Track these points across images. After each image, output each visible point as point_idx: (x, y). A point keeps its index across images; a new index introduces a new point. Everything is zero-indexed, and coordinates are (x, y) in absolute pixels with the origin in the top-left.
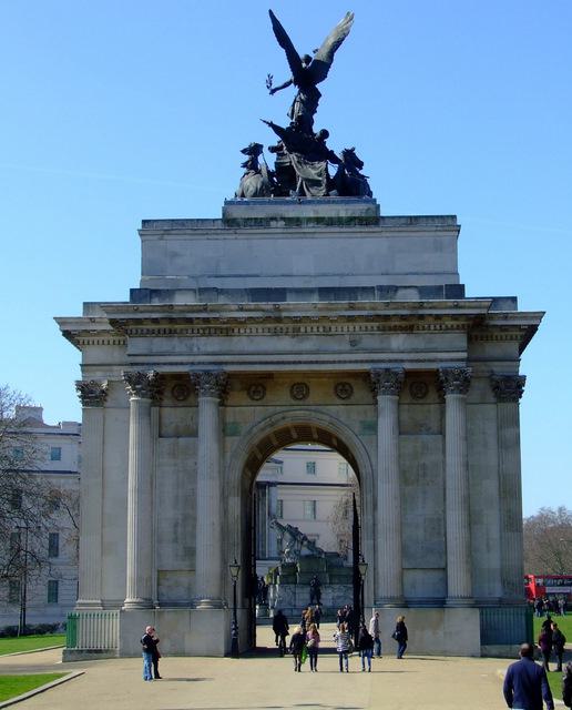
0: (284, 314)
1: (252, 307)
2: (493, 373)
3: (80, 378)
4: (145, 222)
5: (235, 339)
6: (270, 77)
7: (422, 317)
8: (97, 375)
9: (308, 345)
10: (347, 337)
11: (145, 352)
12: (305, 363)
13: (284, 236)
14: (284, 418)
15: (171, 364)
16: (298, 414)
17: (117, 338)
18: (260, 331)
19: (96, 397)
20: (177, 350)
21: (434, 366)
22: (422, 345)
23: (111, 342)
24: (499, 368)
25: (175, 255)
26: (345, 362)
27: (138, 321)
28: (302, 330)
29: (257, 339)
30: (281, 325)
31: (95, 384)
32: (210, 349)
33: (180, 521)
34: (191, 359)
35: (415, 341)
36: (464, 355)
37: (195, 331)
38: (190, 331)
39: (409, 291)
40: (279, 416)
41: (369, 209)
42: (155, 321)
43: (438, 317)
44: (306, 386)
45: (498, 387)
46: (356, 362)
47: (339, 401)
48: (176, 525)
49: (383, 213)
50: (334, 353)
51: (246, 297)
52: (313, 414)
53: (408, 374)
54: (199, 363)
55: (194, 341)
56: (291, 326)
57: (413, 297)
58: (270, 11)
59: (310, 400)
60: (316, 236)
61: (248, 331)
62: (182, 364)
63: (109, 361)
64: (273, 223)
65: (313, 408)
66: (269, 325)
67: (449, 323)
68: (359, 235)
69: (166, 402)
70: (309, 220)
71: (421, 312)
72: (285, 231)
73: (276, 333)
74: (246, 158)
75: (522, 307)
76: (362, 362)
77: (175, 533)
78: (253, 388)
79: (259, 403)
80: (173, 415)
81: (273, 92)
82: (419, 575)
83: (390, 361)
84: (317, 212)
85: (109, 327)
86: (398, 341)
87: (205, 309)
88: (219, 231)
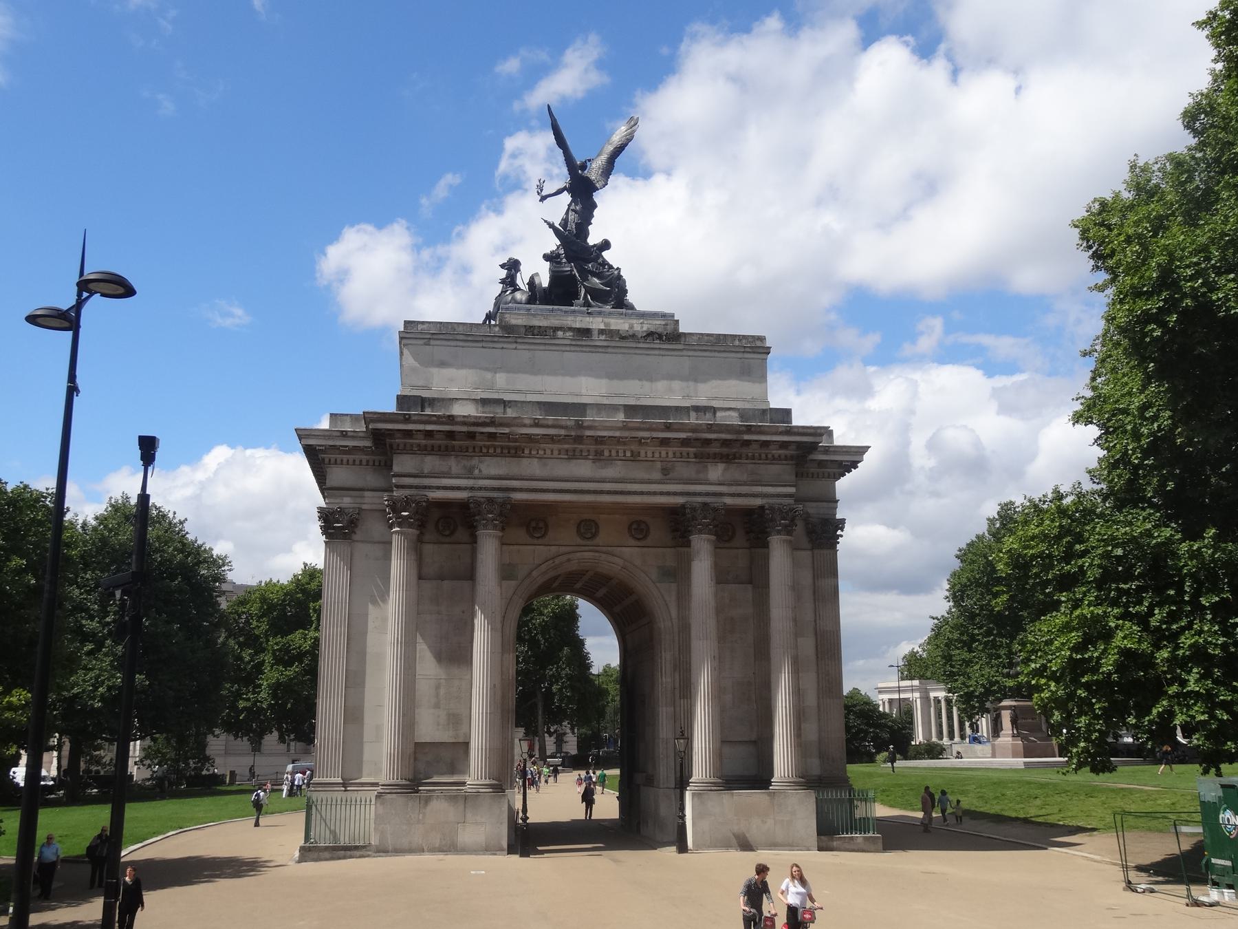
0: (588, 433)
1: (550, 423)
3: (324, 505)
4: (408, 323)
5: (525, 461)
7: (747, 443)
9: (609, 472)
10: (659, 465)
11: (413, 471)
12: (609, 492)
13: (573, 348)
15: (445, 488)
16: (583, 557)
17: (377, 458)
18: (556, 452)
23: (364, 462)
26: (655, 493)
27: (408, 434)
28: (606, 453)
30: (581, 446)
32: (493, 471)
34: (470, 483)
36: (792, 490)
39: (728, 413)
40: (565, 558)
42: (429, 434)
43: (766, 444)
44: (596, 524)
46: (668, 494)
47: (632, 542)
48: (438, 687)
49: (681, 330)
50: (642, 482)
51: (538, 412)
52: (604, 556)
54: (480, 489)
55: (475, 461)
56: (592, 448)
57: (733, 419)
59: (599, 540)
60: (610, 350)
61: (541, 452)
62: (459, 488)
63: (360, 484)
64: (560, 334)
65: (604, 549)
66: (566, 446)
67: (777, 452)
68: (657, 352)
69: (427, 537)
70: (601, 332)
71: (746, 437)
72: (574, 343)
73: (572, 456)
75: (839, 440)
76: (675, 494)
77: (437, 695)
78: (533, 524)
79: (540, 541)
81: (543, 199)
83: (708, 494)
84: (606, 324)
85: (368, 443)
86: (716, 472)
87: (492, 422)
88: (496, 339)
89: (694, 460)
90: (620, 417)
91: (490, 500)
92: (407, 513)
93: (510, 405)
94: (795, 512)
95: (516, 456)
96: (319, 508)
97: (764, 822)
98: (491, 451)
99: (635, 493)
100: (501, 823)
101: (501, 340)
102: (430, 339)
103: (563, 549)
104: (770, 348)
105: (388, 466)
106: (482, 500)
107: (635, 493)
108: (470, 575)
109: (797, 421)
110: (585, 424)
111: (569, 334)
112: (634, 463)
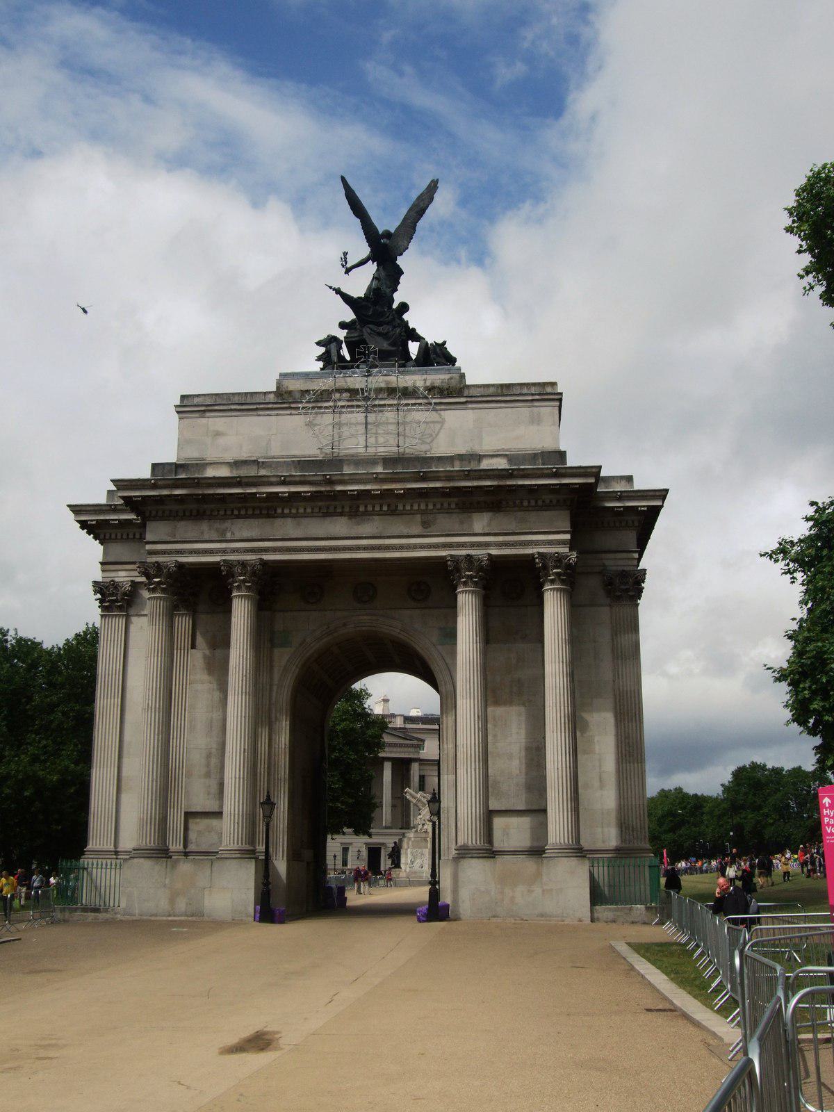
0: (339, 488)
2: (604, 565)
3: (100, 579)
4: (183, 397)
5: (279, 521)
6: (345, 254)
8: (123, 576)
9: (367, 528)
14: (345, 625)
16: (362, 620)
19: (116, 601)
20: (206, 537)
21: (529, 551)
24: (614, 563)
25: (218, 434)
27: (160, 500)
28: (362, 509)
29: (305, 521)
31: (115, 585)
32: (246, 534)
33: (214, 751)
34: (224, 545)
36: (568, 537)
37: (229, 512)
38: (222, 513)
41: (451, 378)
45: (610, 584)
48: (209, 756)
55: (228, 524)
57: (502, 464)
58: (343, 179)
61: (294, 511)
62: (211, 552)
66: (320, 504)
70: (379, 391)
72: (350, 404)
74: (323, 350)
75: (638, 485)
77: (208, 765)
81: (348, 271)
82: (514, 821)
84: (387, 383)
88: (270, 406)
89: (457, 510)
91: (243, 564)
92: (158, 580)
93: (264, 466)
94: (569, 560)
95: (268, 516)
96: (96, 584)
97: (530, 892)
98: (243, 512)
100: (248, 889)
101: (275, 406)
102: (204, 411)
104: (561, 394)
106: (235, 563)
109: (572, 461)
110: (334, 478)
111: (345, 395)
112: (395, 517)
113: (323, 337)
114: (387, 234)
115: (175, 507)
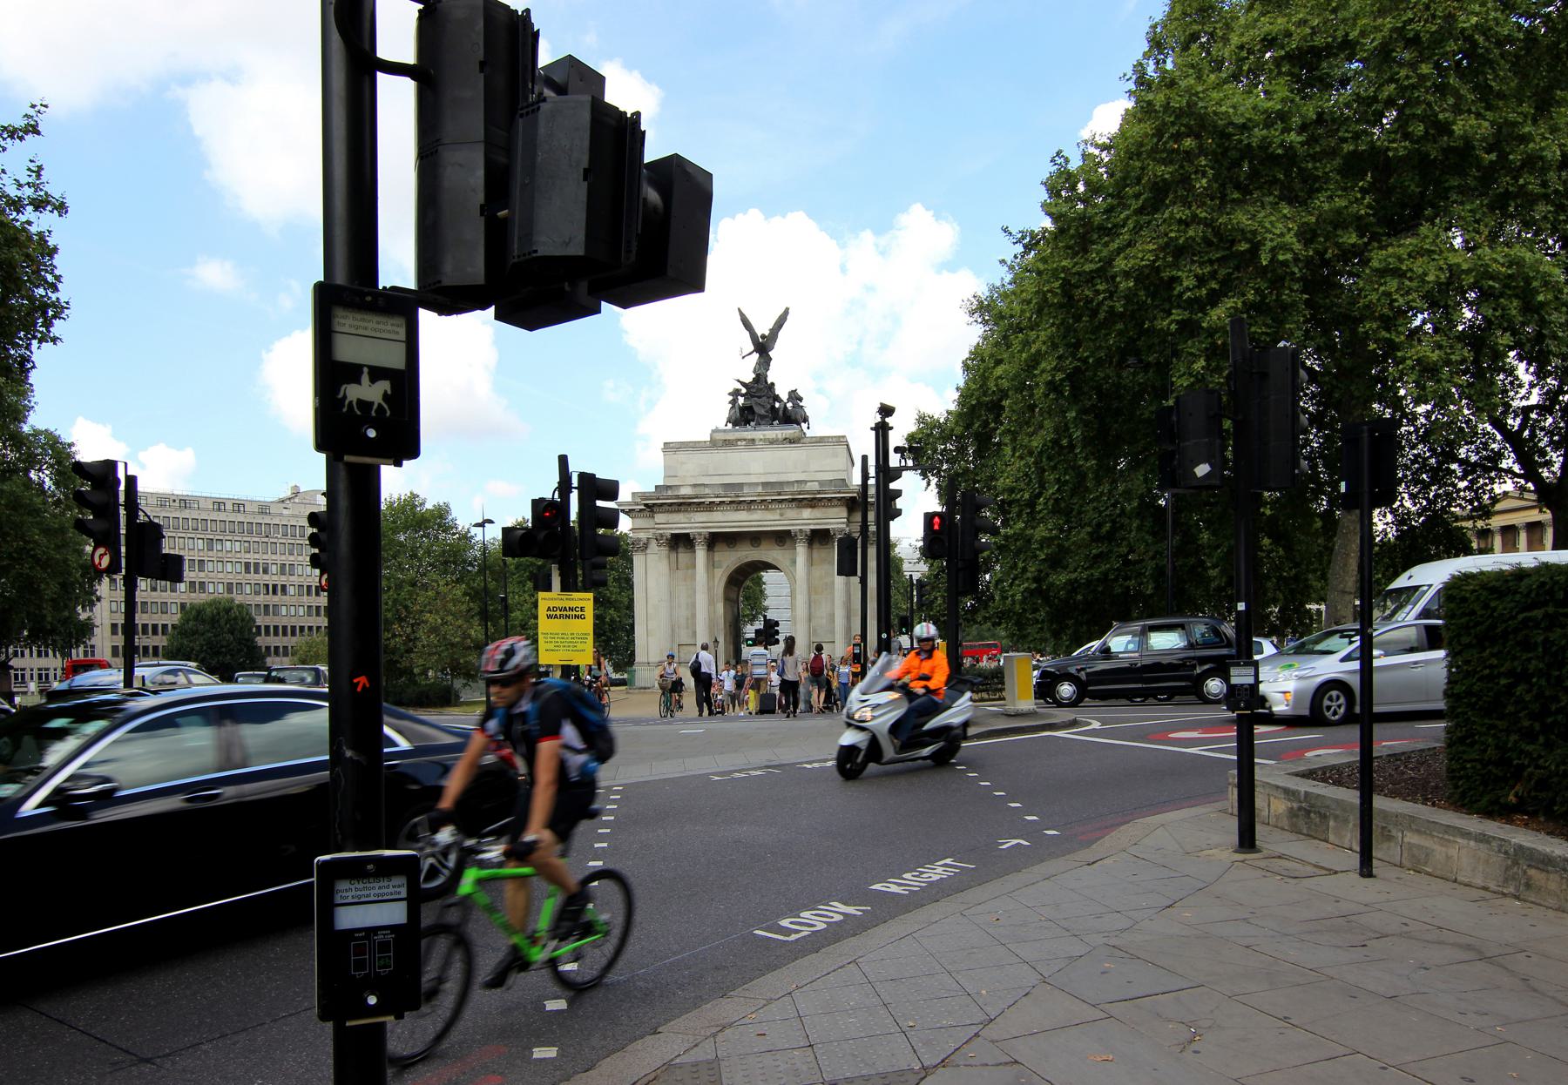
22: (819, 516)
25: (682, 463)
31: (639, 540)
32: (701, 520)
35: (817, 513)
48: (687, 619)
53: (812, 531)
57: (815, 486)
58: (739, 309)
62: (685, 528)
64: (739, 443)
69: (680, 550)
74: (731, 398)
80: (683, 556)
83: (803, 524)
90: (760, 489)
99: (768, 526)
103: (744, 553)
105: (653, 517)
107: (768, 526)
108: (694, 566)
111: (744, 443)
113: (731, 390)
114: (763, 336)
115: (667, 508)
